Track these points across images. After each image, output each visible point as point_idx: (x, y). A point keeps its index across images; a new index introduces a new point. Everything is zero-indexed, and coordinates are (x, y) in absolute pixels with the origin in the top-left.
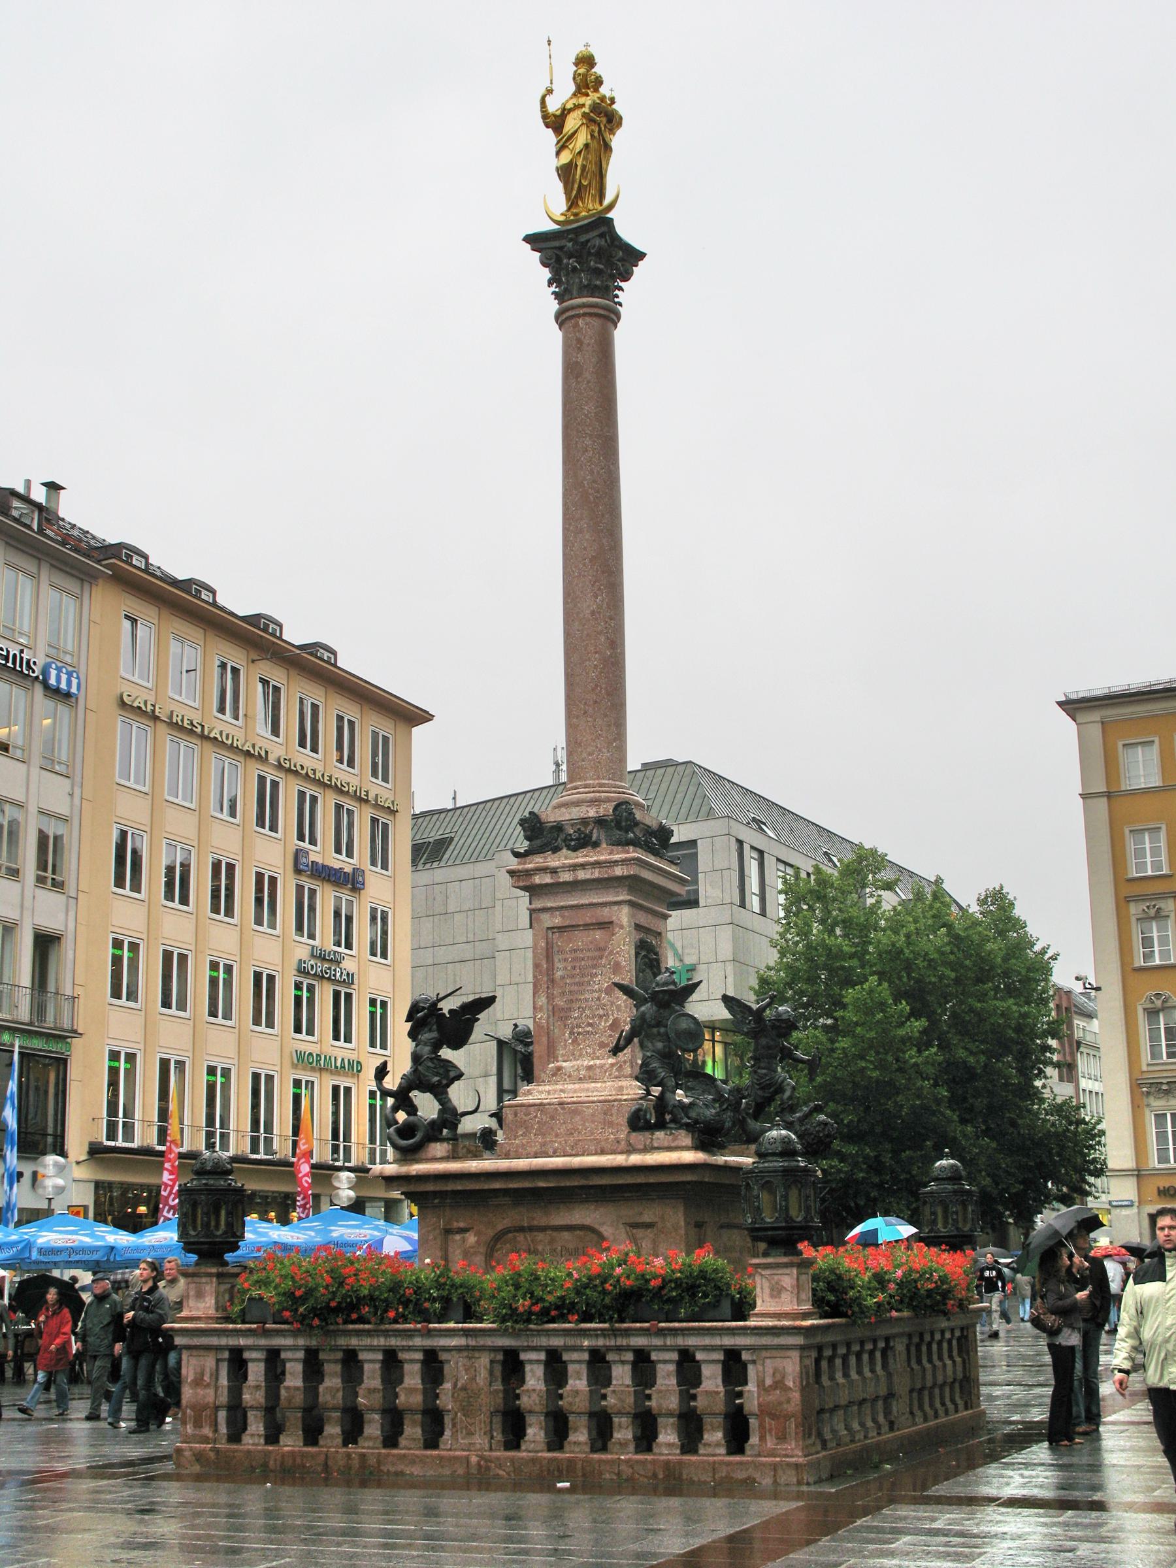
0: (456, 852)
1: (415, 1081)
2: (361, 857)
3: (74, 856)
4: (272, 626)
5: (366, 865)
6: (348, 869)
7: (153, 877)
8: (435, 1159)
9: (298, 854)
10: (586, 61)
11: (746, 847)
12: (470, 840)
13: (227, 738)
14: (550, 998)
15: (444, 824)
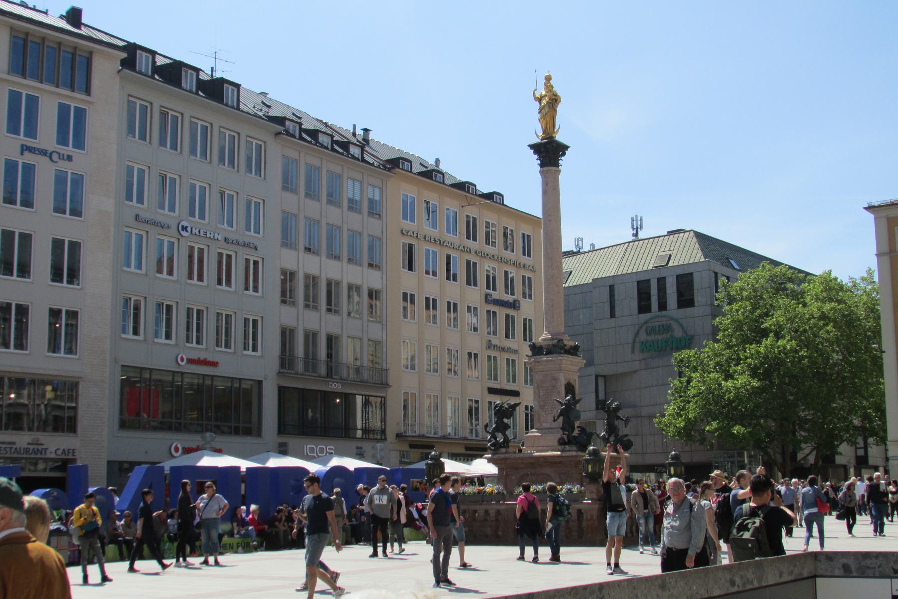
0: (573, 279)
1: (497, 429)
2: (518, 294)
3: (384, 294)
4: (471, 187)
5: (521, 298)
6: (511, 301)
7: (420, 302)
8: (502, 453)
9: (487, 296)
10: (548, 79)
11: (719, 275)
12: (580, 272)
13: (452, 245)
14: (539, 402)
15: (568, 264)
